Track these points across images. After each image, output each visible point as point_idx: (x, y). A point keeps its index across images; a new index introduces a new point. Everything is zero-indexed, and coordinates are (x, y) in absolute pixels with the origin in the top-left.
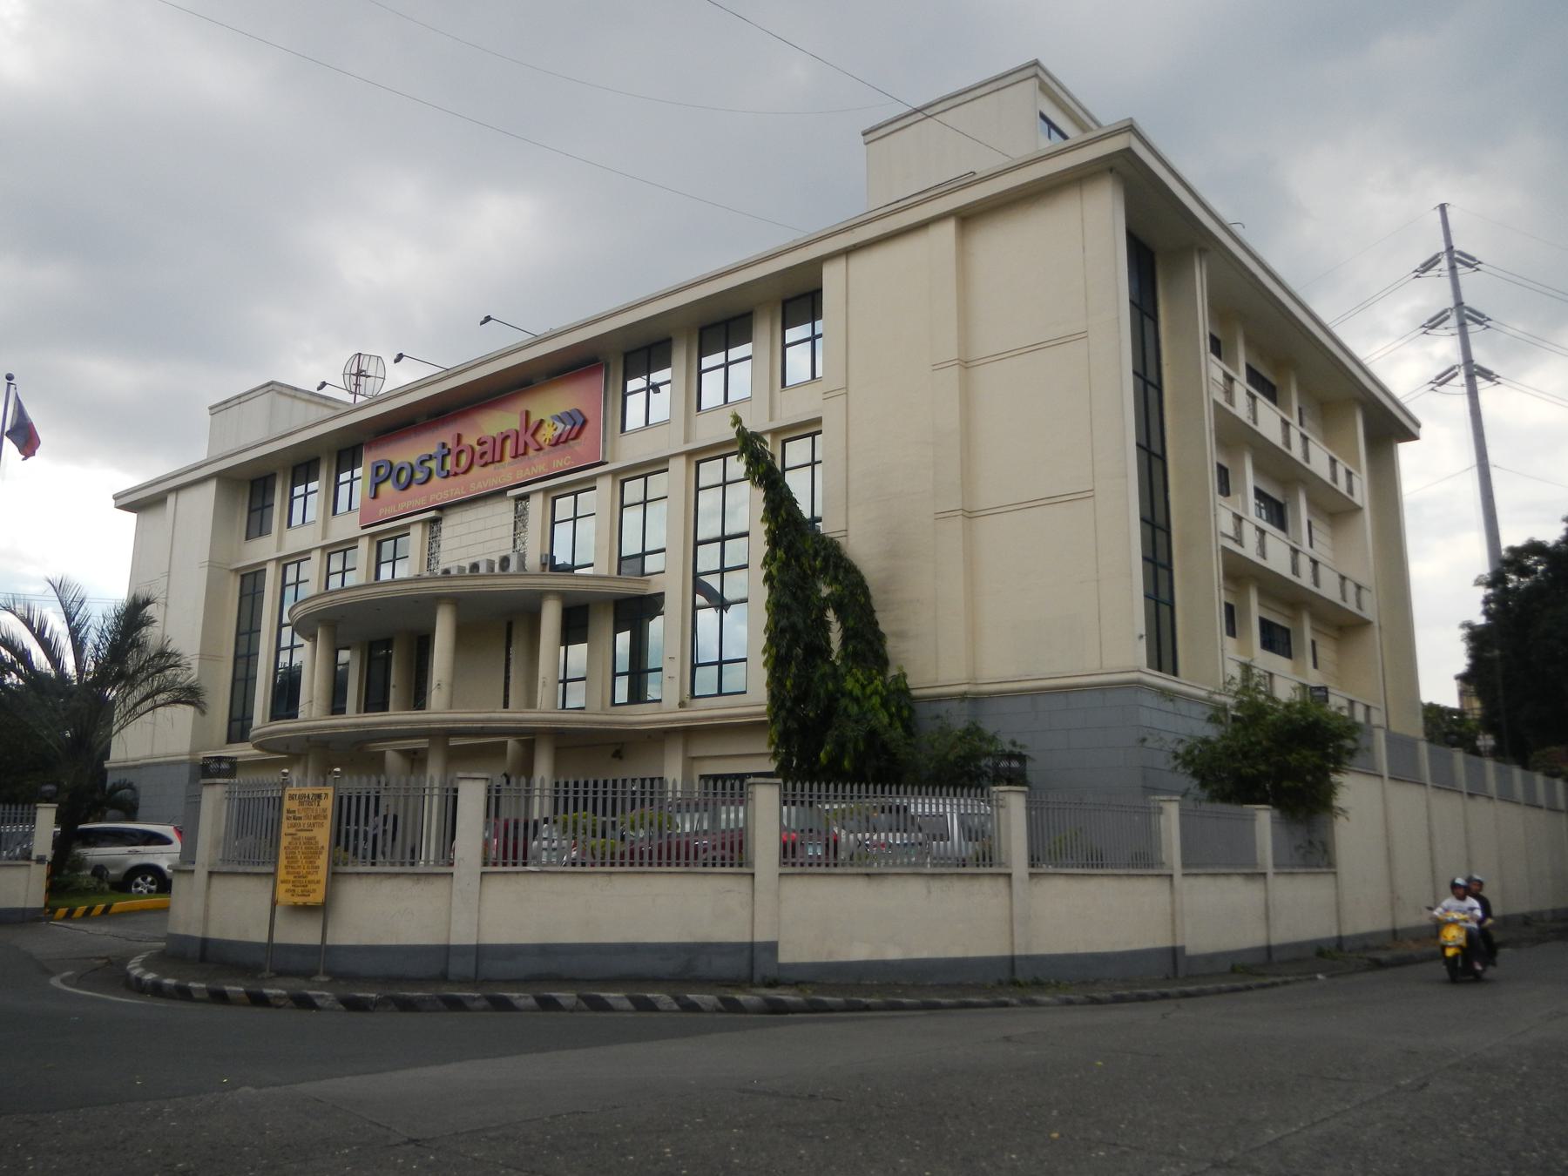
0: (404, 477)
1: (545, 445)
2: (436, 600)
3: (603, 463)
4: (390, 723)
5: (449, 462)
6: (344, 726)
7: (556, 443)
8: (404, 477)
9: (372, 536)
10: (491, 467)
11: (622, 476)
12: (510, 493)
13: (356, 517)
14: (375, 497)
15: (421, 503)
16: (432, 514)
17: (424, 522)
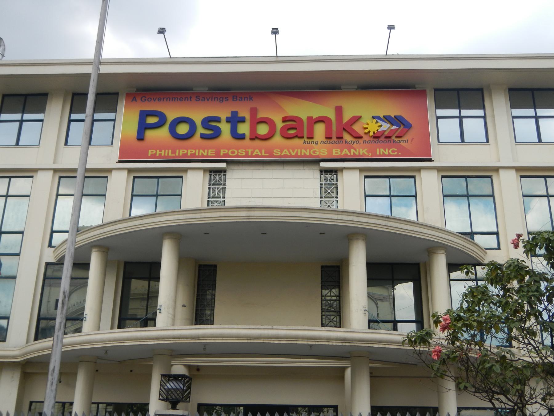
0: (183, 129)
1: (366, 138)
2: (350, 235)
3: (430, 160)
4: (380, 342)
5: (244, 129)
6: (328, 339)
7: (376, 137)
8: (183, 129)
9: (130, 170)
10: (297, 142)
11: (447, 173)
12: (322, 165)
13: (114, 152)
14: (140, 137)
15: (210, 153)
16: (223, 165)
17: (205, 170)
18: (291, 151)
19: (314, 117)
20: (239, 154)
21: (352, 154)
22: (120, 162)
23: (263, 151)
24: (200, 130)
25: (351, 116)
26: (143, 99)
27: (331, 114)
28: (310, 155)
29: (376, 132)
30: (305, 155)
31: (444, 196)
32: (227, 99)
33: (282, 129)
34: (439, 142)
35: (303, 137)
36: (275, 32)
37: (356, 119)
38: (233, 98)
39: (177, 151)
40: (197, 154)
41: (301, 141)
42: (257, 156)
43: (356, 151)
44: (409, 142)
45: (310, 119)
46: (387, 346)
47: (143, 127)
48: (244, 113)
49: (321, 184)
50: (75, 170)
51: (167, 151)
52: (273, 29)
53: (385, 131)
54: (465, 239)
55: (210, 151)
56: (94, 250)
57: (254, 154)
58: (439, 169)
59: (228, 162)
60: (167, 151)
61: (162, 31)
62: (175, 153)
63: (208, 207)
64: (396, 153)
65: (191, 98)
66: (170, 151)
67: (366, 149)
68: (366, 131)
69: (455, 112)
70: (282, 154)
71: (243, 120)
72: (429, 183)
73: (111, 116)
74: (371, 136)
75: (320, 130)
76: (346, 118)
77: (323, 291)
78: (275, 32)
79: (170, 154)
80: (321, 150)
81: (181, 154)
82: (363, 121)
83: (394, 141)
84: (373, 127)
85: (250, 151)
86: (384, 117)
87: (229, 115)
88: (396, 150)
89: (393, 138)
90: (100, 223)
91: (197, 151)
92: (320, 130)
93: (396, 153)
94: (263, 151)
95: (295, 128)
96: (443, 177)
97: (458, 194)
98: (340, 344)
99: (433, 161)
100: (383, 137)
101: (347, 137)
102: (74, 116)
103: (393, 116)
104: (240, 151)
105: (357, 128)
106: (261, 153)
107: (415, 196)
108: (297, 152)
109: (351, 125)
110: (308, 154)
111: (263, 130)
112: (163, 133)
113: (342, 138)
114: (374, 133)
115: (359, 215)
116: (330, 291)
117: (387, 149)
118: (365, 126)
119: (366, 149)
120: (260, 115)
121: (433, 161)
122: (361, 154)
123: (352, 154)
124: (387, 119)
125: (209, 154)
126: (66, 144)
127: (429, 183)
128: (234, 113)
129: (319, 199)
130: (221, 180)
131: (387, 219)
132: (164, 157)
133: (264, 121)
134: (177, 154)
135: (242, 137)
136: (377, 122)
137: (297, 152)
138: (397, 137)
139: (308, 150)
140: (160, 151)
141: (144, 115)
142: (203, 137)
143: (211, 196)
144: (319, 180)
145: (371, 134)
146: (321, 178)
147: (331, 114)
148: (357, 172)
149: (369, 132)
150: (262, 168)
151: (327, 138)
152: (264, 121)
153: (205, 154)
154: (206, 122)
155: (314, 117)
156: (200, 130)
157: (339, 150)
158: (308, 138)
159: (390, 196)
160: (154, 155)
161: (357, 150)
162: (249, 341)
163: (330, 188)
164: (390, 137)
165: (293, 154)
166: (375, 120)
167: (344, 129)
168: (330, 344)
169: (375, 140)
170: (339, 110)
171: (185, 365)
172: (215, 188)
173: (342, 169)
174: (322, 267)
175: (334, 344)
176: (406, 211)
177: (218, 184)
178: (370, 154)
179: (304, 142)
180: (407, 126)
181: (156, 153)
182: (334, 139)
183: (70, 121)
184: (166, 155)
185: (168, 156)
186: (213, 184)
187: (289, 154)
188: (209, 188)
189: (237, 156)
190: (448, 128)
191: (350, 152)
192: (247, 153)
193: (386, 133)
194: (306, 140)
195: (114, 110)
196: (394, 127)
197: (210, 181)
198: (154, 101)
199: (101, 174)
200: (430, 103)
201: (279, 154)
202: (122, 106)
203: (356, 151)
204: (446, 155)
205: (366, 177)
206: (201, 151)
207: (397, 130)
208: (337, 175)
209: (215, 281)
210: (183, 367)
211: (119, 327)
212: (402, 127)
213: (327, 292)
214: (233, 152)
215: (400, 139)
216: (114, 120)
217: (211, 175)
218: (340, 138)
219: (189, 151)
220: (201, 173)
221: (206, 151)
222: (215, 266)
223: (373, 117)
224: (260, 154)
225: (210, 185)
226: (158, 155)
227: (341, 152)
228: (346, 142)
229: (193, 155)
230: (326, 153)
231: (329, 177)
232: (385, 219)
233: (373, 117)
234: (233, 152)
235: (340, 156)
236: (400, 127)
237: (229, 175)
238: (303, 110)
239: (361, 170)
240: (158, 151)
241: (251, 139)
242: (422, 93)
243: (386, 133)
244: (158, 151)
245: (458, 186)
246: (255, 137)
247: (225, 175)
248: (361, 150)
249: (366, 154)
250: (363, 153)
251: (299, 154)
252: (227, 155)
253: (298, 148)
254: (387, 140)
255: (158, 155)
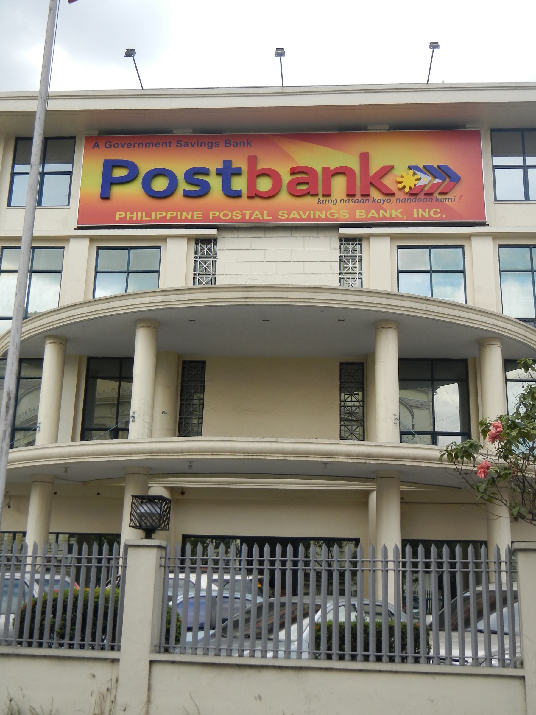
0: (160, 184)
1: (400, 195)
2: (377, 322)
3: (484, 224)
4: (414, 458)
5: (239, 184)
6: (348, 455)
7: (414, 193)
8: (160, 184)
9: (92, 239)
10: (309, 200)
11: (506, 242)
12: (343, 231)
14: (105, 196)
15: (197, 216)
16: (213, 232)
17: (189, 238)
18: (301, 212)
19: (332, 168)
20: (234, 217)
21: (381, 216)
22: (79, 228)
23: (265, 213)
24: (183, 186)
25: (381, 166)
26: (107, 146)
27: (354, 164)
28: (327, 219)
29: (413, 187)
30: (320, 219)
31: (501, 271)
32: (217, 145)
33: (290, 183)
34: (495, 200)
35: (317, 195)
36: (280, 53)
37: (387, 170)
38: (226, 143)
39: (154, 213)
40: (179, 218)
41: (315, 200)
42: (257, 219)
43: (386, 212)
44: (456, 201)
45: (326, 170)
46: (423, 464)
47: (109, 182)
48: (240, 162)
49: (340, 257)
50: (18, 239)
51: (139, 213)
52: (277, 49)
53: (425, 186)
54: (528, 327)
55: (195, 213)
56: (48, 341)
57: (253, 218)
58: (495, 236)
59: (219, 228)
60: (139, 213)
61: (130, 53)
62: (151, 217)
63: (194, 287)
64: (439, 215)
65: (170, 143)
66: (144, 213)
67: (400, 210)
68: (400, 186)
69: (518, 160)
70: (290, 218)
71: (238, 172)
72: (482, 255)
73: (66, 167)
74: (407, 193)
75: (339, 185)
76: (374, 168)
77: (343, 395)
78: (280, 53)
79: (144, 218)
80: (340, 211)
81: (158, 218)
82: (397, 172)
83: (437, 200)
84: (410, 181)
85: (247, 213)
86: (424, 166)
87: (220, 166)
88: (439, 210)
89: (436, 194)
90: (55, 306)
91: (179, 213)
92: (339, 185)
93: (439, 215)
94: (265, 213)
95: (306, 183)
96: (500, 246)
97: (520, 268)
98: (363, 461)
99: (488, 225)
100: (423, 193)
101: (375, 194)
102: (18, 168)
103: (436, 166)
104: (234, 213)
105: (388, 181)
106: (263, 216)
107: (463, 272)
108: (309, 214)
109: (381, 178)
110: (323, 216)
111: (264, 185)
112: (135, 189)
113: (368, 195)
114: (410, 188)
115: (390, 296)
116: (352, 395)
117: (427, 210)
118: (399, 179)
119: (400, 210)
120: (262, 165)
121: (488, 225)
122: (393, 216)
123: (381, 216)
124: (428, 170)
125: (195, 218)
126: (9, 204)
127: (482, 255)
128: (227, 164)
129: (338, 277)
130: (210, 251)
131: (425, 302)
132: (137, 221)
133: (266, 173)
134: (153, 218)
135: (237, 195)
136: (414, 174)
137: (309, 214)
138: (440, 194)
139: (324, 212)
140: (132, 213)
141: (109, 166)
142: (187, 195)
143: (198, 272)
144: (338, 250)
145: (407, 190)
146: (340, 248)
147: (354, 164)
148: (388, 241)
149: (404, 187)
150: (263, 235)
151: (348, 195)
152: (266, 173)
153: (190, 217)
154: (191, 175)
155: (332, 168)
156: (183, 186)
157: (364, 212)
158: (323, 195)
159: (431, 272)
160: (122, 219)
161: (388, 211)
162: (247, 457)
163: (352, 261)
164: (431, 194)
165: (304, 217)
166: (412, 172)
167: (371, 183)
168: (350, 461)
169: (412, 198)
170: (365, 159)
171: (165, 487)
172: (203, 262)
173: (368, 237)
174: (341, 364)
175: (356, 461)
176: (450, 291)
177: (206, 257)
178: (405, 217)
179: (319, 202)
180: (455, 179)
181: (126, 216)
182: (358, 197)
183: (13, 174)
184: (139, 218)
185: (142, 221)
186: (200, 257)
187: (298, 217)
188: (195, 262)
189: (231, 220)
190: (508, 182)
191: (379, 214)
192: (244, 215)
193: (426, 189)
194: (321, 198)
195: (71, 160)
196: (437, 181)
197: (196, 253)
198: (123, 147)
199: (56, 244)
200: (485, 147)
201: (286, 216)
202: (80, 154)
203: (386, 212)
204: (505, 218)
205: (399, 247)
206: (184, 213)
207: (442, 184)
208: (361, 244)
209: (204, 381)
210: (163, 489)
211: (82, 439)
212: (448, 180)
213: (346, 396)
214: (225, 215)
215: (445, 197)
216: (70, 173)
217: (197, 245)
218: (366, 195)
219: (169, 213)
220: (185, 242)
221: (191, 213)
222: (204, 363)
223: (410, 168)
224: (261, 218)
225: (196, 257)
226: (128, 218)
227: (367, 214)
228: (374, 201)
229: (174, 219)
230: (348, 216)
231: (350, 247)
232: (423, 301)
233: (410, 168)
234: (225, 215)
235: (366, 219)
236: (444, 180)
237: (220, 245)
238: (317, 158)
239: (393, 237)
240: (128, 213)
241: (249, 197)
242: (475, 135)
243: (426, 189)
244: (128, 213)
245: (520, 258)
246: (254, 195)
247: (216, 245)
248: (393, 211)
249: (400, 216)
250: (396, 215)
251: (312, 217)
252: (218, 218)
253: (310, 209)
254: (428, 197)
255: (128, 218)
